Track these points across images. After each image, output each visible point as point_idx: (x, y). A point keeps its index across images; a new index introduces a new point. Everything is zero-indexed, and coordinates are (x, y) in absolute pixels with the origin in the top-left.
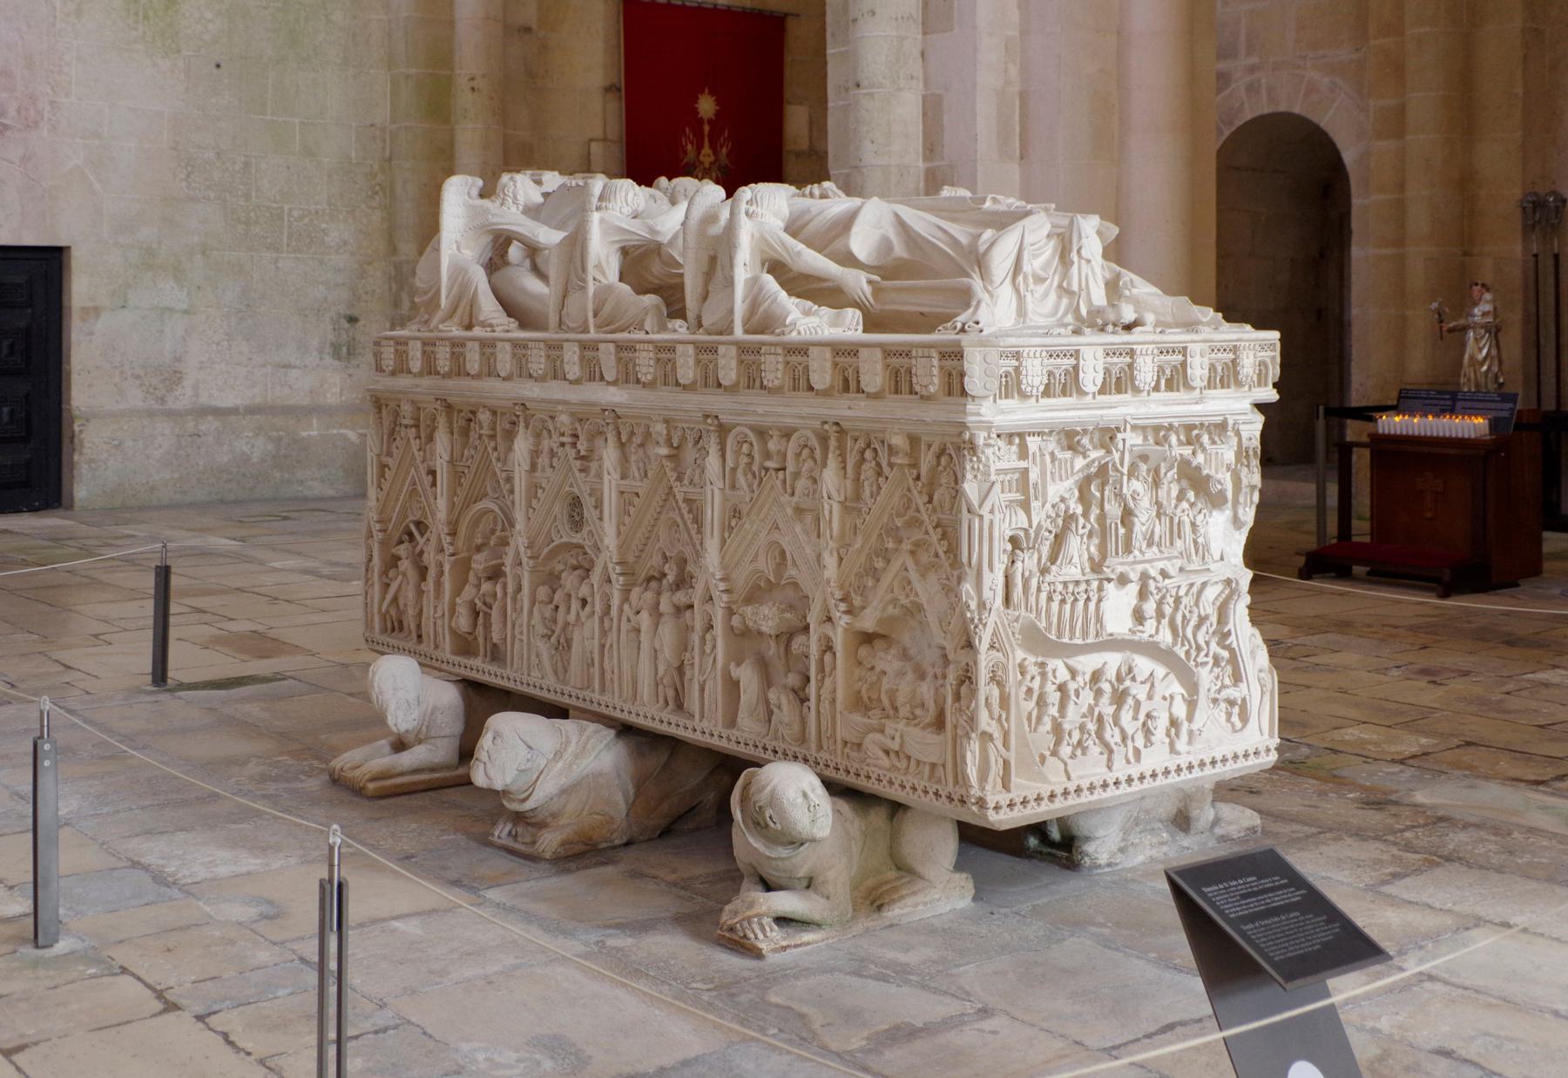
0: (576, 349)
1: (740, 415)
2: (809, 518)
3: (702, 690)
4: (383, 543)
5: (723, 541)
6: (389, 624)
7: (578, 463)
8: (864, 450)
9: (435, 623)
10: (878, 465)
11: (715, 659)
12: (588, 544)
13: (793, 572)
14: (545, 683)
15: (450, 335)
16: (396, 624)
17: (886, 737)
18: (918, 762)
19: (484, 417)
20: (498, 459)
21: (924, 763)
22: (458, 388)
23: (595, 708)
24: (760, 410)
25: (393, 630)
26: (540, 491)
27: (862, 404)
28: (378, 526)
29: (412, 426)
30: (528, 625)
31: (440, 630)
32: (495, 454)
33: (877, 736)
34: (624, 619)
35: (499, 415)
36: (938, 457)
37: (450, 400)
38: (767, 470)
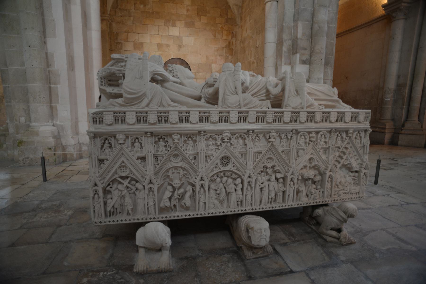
0: (237, 113)
1: (306, 129)
2: (322, 151)
3: (288, 195)
4: (103, 188)
5: (296, 160)
6: (108, 214)
7: (232, 147)
8: (338, 135)
9: (148, 208)
10: (342, 138)
11: (294, 187)
12: (234, 169)
13: (317, 163)
14: (218, 211)
15: (157, 110)
16: (112, 214)
17: (345, 191)
18: (351, 193)
19: (176, 137)
20: (184, 150)
21: (353, 193)
22: (163, 127)
23: (244, 212)
24: (314, 127)
25: (110, 215)
26: (211, 157)
27: (344, 125)
28: (102, 182)
29: (124, 144)
30: (209, 197)
31: (152, 209)
32: (183, 149)
33: (344, 191)
34: (257, 186)
35: (183, 136)
36: (357, 135)
37: (154, 132)
38: (311, 141)
